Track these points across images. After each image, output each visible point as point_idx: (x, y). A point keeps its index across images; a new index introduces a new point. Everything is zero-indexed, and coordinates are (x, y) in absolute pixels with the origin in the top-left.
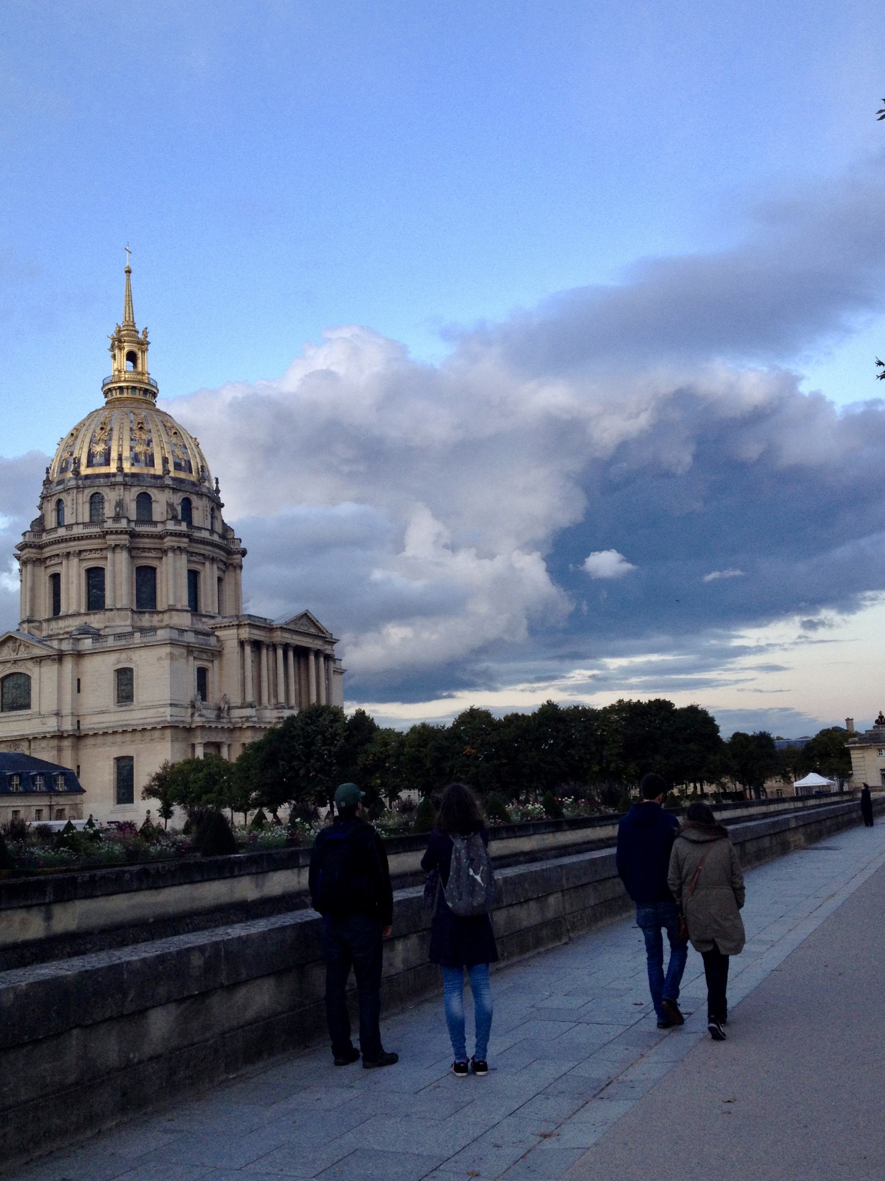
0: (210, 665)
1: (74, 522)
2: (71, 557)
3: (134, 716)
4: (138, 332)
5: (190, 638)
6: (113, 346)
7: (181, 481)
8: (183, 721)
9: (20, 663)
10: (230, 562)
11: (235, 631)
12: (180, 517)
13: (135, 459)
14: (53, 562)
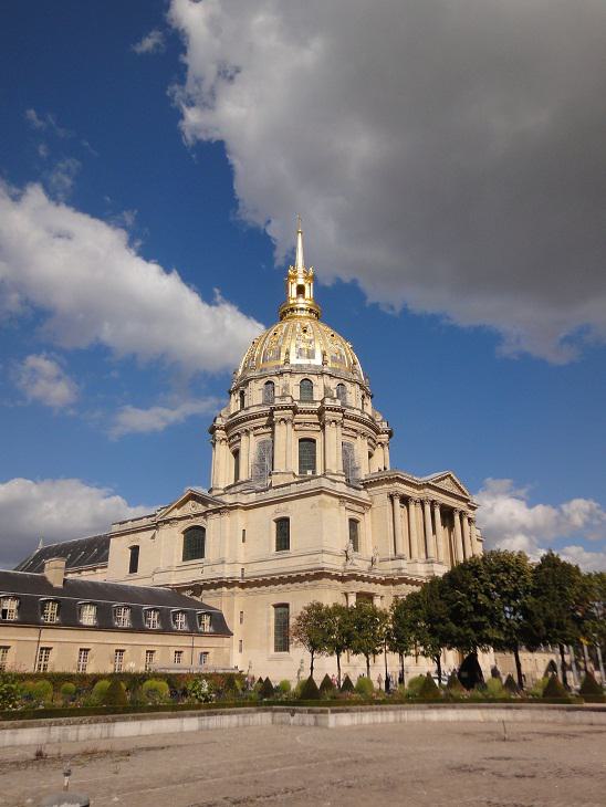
3: (291, 563)
10: (378, 440)
13: (300, 353)
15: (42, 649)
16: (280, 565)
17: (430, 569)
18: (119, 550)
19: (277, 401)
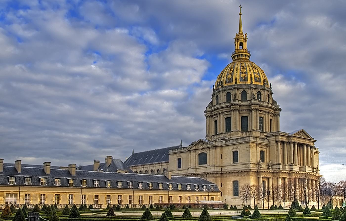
0: (265, 150)
1: (221, 102)
2: (220, 115)
4: (244, 35)
5: (258, 141)
6: (235, 42)
7: (257, 85)
8: (255, 170)
9: (204, 149)
10: (275, 113)
11: (274, 137)
12: (256, 98)
14: (215, 116)
15: (170, 196)
16: (236, 168)
17: (291, 168)
18: (173, 159)
19: (232, 102)
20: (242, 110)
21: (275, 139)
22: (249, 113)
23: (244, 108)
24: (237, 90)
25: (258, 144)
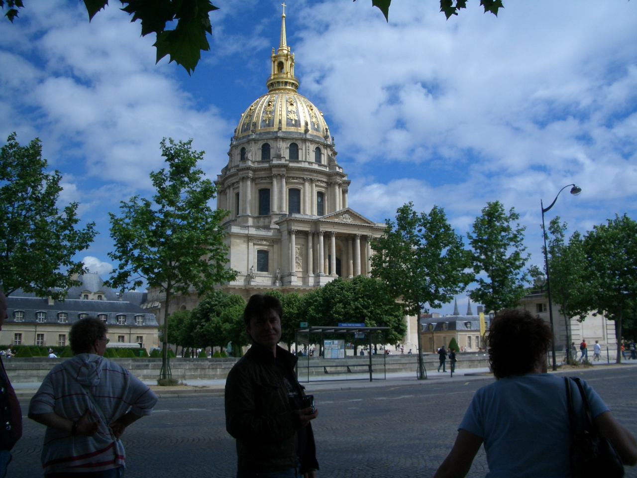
0: (271, 248)
7: (290, 133)
11: (286, 225)
15: (38, 335)
20: (259, 178)
21: (285, 229)
22: (272, 183)
23: (262, 174)
24: (253, 143)
25: (250, 238)
